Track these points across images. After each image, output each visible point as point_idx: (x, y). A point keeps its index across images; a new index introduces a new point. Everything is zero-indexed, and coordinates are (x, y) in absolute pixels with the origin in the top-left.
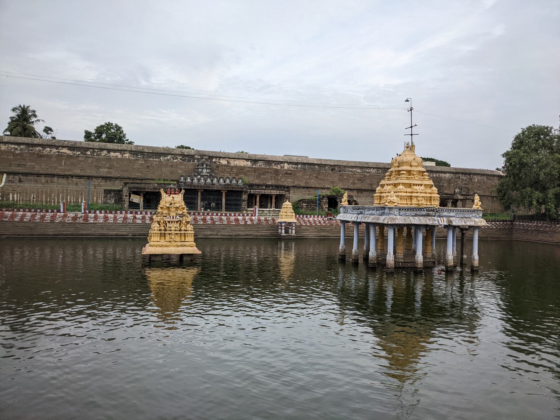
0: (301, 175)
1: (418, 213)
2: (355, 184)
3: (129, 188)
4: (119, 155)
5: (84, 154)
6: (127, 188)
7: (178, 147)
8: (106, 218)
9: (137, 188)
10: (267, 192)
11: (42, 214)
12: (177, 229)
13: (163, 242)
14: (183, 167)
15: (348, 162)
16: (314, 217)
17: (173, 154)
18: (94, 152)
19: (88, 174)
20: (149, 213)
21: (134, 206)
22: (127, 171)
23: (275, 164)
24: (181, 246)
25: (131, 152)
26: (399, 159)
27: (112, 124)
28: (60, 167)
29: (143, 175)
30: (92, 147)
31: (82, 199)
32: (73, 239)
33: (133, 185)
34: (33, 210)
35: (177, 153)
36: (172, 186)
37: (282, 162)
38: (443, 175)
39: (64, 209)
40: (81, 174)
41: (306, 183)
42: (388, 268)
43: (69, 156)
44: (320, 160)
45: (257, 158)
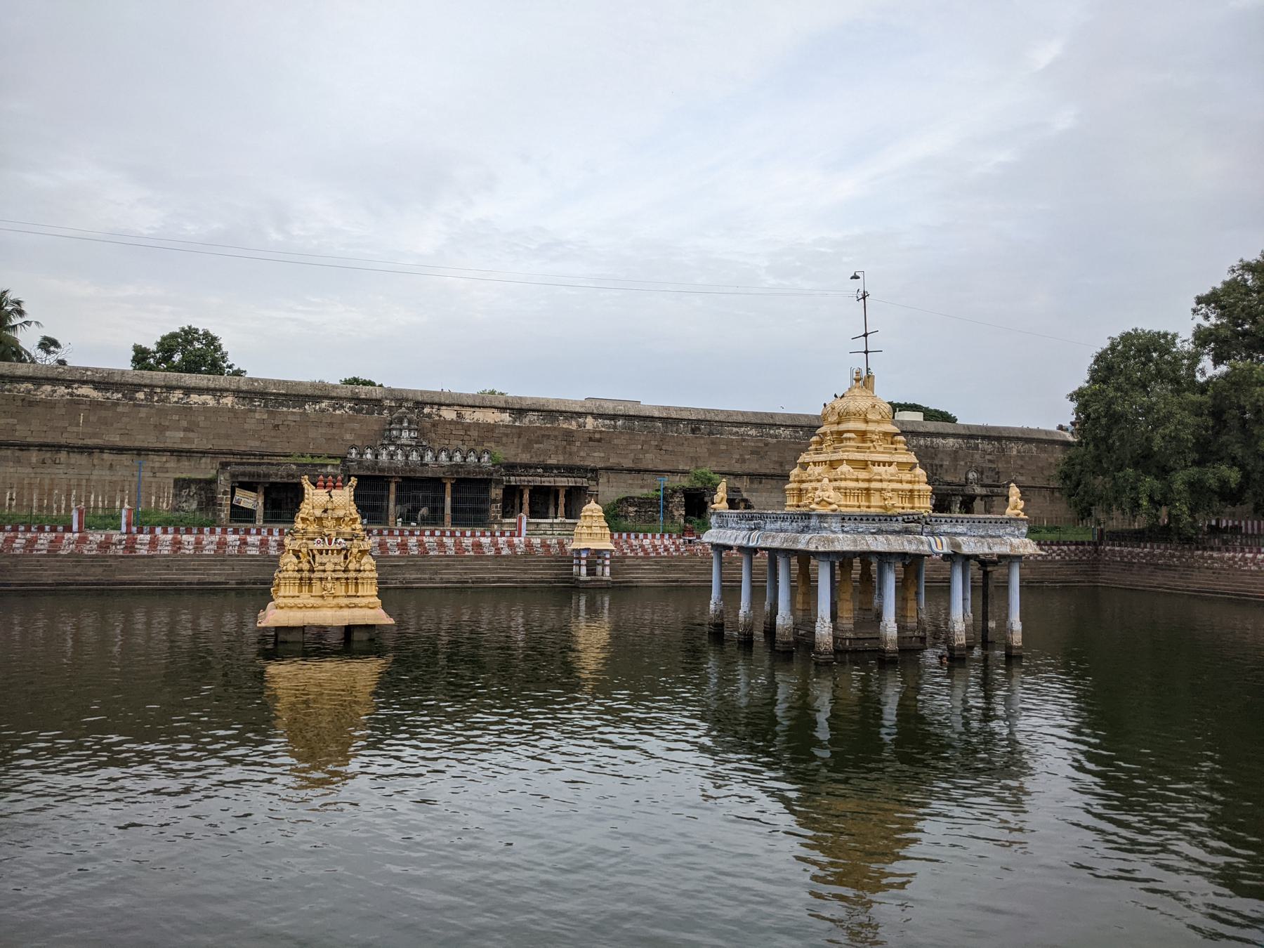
1: (884, 526)
2: (744, 461)
3: (233, 475)
4: (209, 399)
5: (131, 399)
6: (227, 475)
7: (348, 382)
8: (177, 544)
9: (251, 475)
10: (547, 481)
11: (29, 535)
12: (338, 567)
13: (305, 598)
14: (357, 426)
15: (729, 413)
16: (654, 537)
17: (332, 398)
18: (152, 393)
19: (137, 444)
20: (276, 532)
21: (241, 515)
22: (228, 436)
23: (566, 418)
24: (348, 607)
25: (237, 393)
26: (840, 405)
27: (196, 331)
28: (75, 429)
29: (264, 445)
30: (148, 382)
31: (122, 502)
32: (101, 593)
33: (241, 468)
34: (8, 527)
35: (343, 395)
36: (329, 469)
37: (580, 414)
38: (940, 441)
39: (80, 523)
40: (121, 444)
41: (635, 460)
42: (821, 654)
43: (95, 404)
44: (667, 408)
45: (525, 405)
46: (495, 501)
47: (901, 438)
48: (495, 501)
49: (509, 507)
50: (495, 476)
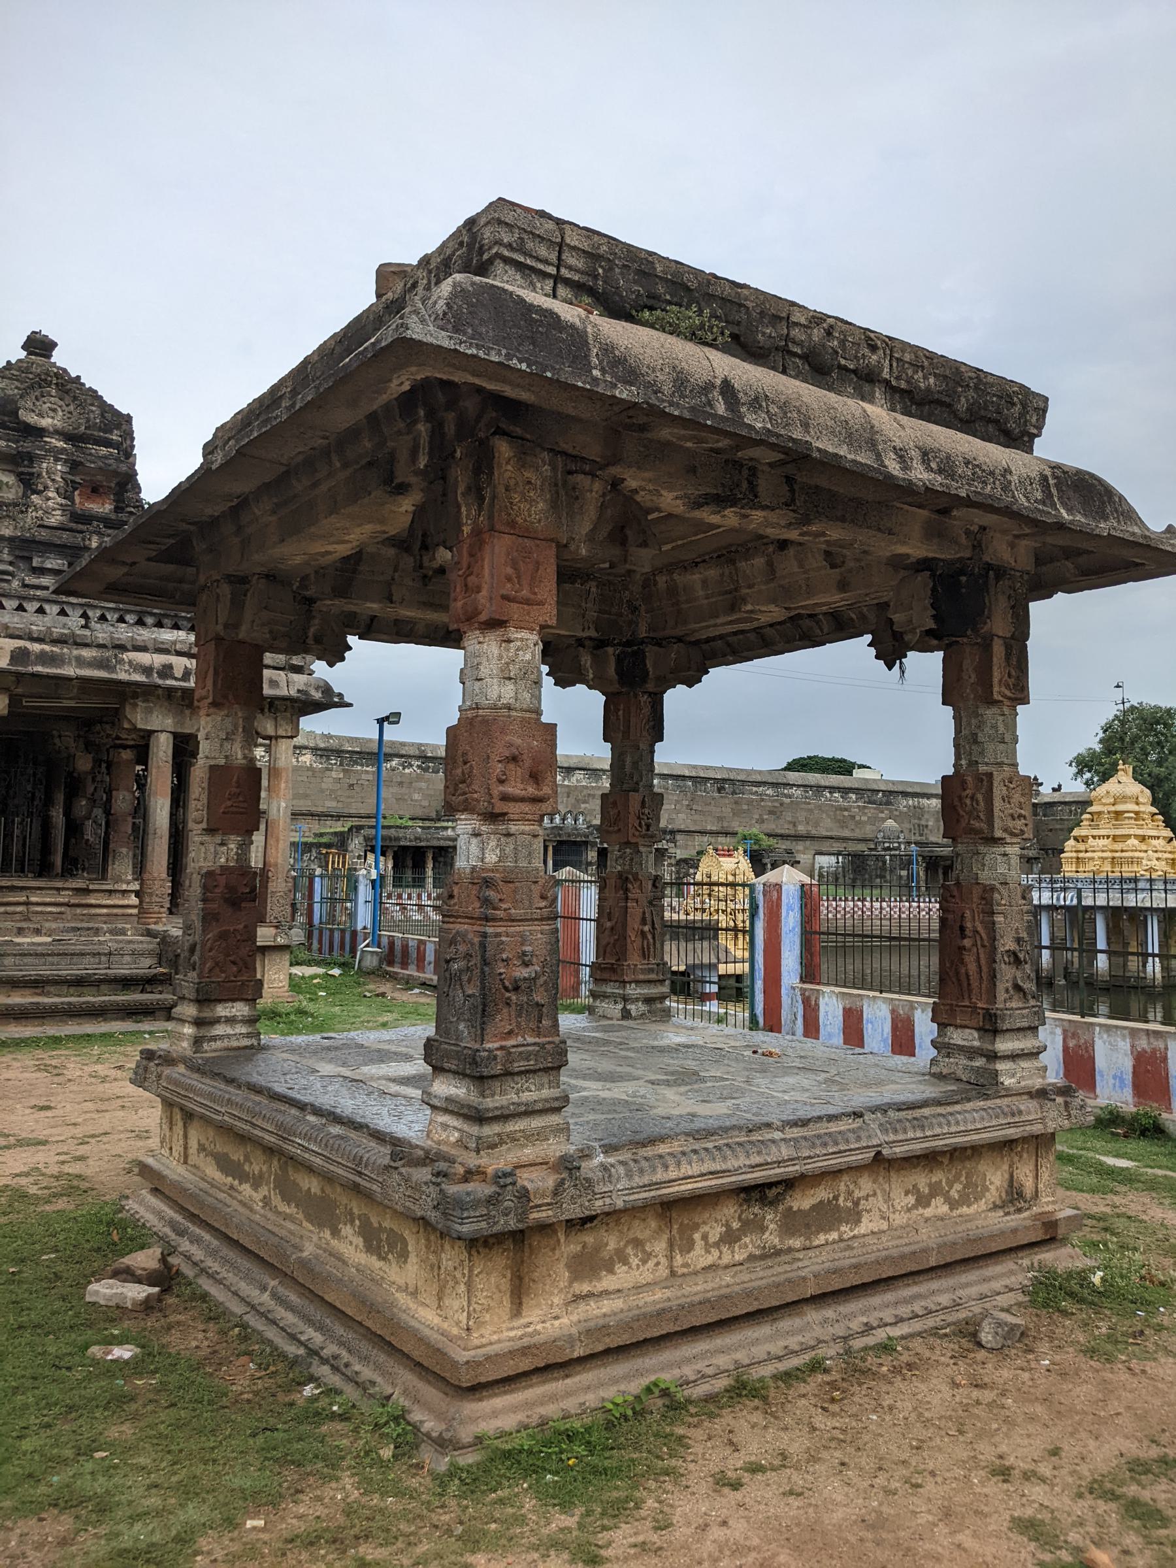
2: (763, 821)
6: (361, 839)
14: (423, 785)
15: (749, 772)
17: (402, 756)
22: (306, 796)
25: (315, 750)
29: (340, 805)
35: (411, 753)
38: (925, 801)
44: (695, 767)
46: (590, 864)
47: (1160, 817)
48: (590, 864)
50: (591, 838)
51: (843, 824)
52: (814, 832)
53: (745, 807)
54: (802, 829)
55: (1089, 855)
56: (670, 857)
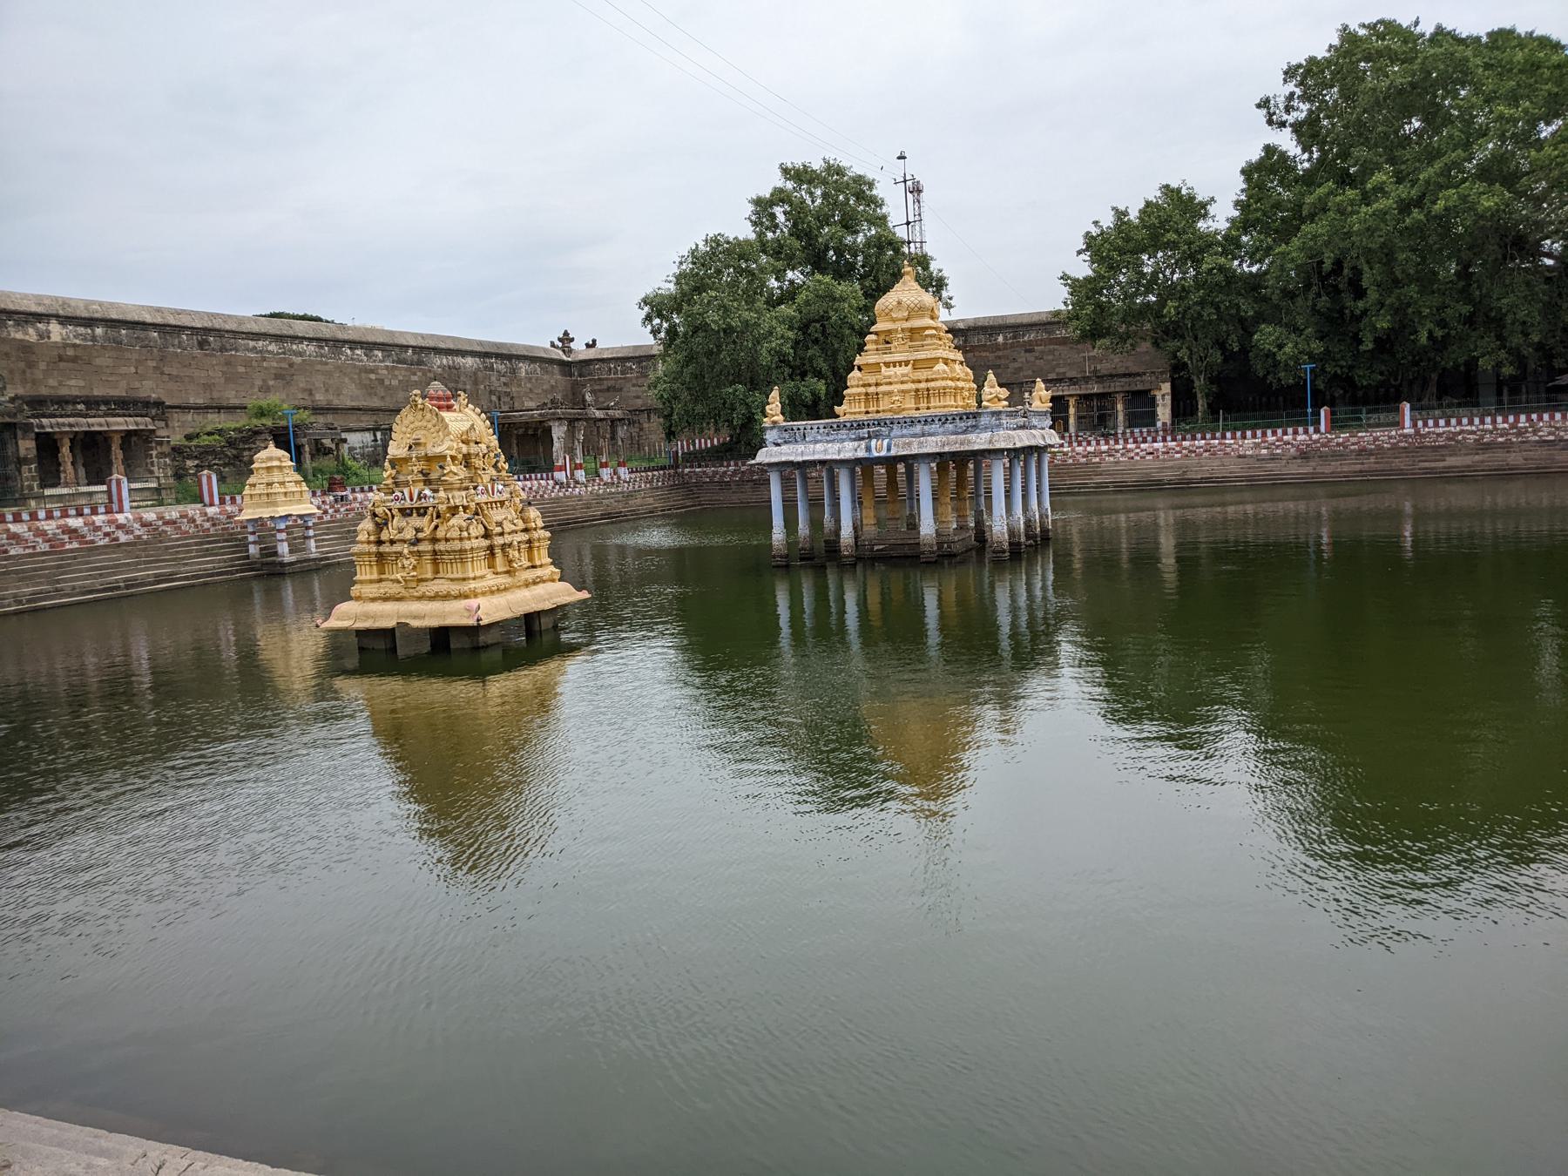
0: (109, 362)
2: (265, 389)
10: (96, 423)
13: (492, 581)
23: (18, 324)
38: (460, 360)
44: (158, 310)
46: (26, 461)
48: (26, 461)
49: (50, 476)
50: (19, 419)
51: (370, 389)
52: (336, 402)
53: (241, 369)
54: (320, 398)
55: (881, 389)
56: (161, 443)
